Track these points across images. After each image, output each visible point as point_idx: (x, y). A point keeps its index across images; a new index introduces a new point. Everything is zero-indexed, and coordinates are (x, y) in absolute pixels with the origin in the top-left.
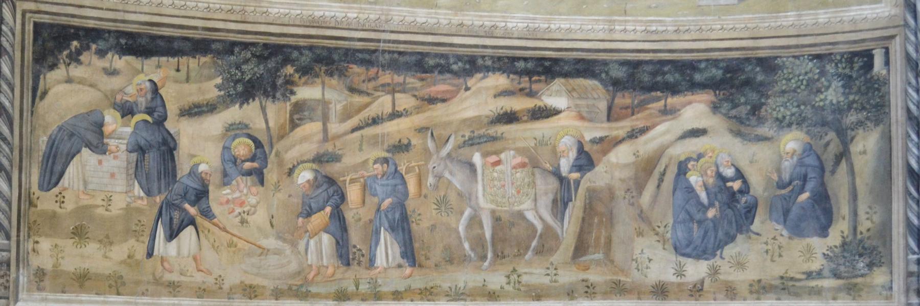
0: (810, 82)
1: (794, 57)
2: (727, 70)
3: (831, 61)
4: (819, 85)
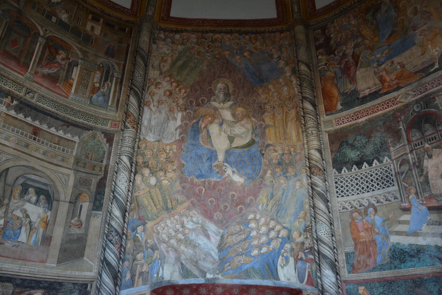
0: (71, 290)
1: (68, 283)
2: (49, 284)
3: (77, 285)
4: (73, 291)
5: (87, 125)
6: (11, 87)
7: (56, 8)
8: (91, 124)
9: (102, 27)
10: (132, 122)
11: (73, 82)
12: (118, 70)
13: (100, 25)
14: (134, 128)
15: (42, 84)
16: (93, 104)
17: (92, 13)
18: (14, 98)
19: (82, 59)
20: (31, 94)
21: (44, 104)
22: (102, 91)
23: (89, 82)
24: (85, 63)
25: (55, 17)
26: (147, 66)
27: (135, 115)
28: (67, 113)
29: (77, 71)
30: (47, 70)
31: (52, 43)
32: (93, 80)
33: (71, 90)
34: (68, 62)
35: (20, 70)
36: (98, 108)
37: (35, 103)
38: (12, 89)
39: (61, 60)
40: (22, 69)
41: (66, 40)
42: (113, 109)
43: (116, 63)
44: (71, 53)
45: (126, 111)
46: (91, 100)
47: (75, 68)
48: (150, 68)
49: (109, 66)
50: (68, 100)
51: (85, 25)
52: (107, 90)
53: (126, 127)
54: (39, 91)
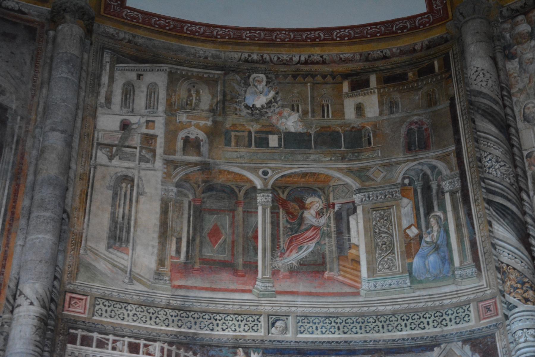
5: (422, 338)
6: (237, 328)
7: (270, 114)
8: (431, 331)
9: (379, 93)
10: (517, 288)
11: (358, 251)
12: (448, 172)
13: (374, 92)
14: (527, 300)
15: (295, 290)
16: (420, 282)
17: (345, 76)
18: (249, 348)
19: (359, 191)
20: (279, 324)
21: (312, 333)
22: (428, 239)
23: (392, 236)
24: (369, 197)
25: (274, 134)
26: (509, 126)
27: (519, 267)
28: (368, 329)
29: (357, 223)
30: (296, 255)
31: (286, 193)
32: (400, 225)
33: (360, 271)
34: (332, 214)
35: (243, 284)
36: (433, 284)
37: (294, 340)
38: (240, 333)
39: (316, 217)
40: (245, 279)
41: (313, 170)
42: (469, 271)
43: (438, 158)
44: (333, 191)
45: (497, 265)
46: (410, 274)
47: (351, 218)
48: (521, 125)
49: (425, 175)
50: (361, 299)
51: (340, 112)
52: (439, 232)
53: (511, 307)
54: (293, 309)
